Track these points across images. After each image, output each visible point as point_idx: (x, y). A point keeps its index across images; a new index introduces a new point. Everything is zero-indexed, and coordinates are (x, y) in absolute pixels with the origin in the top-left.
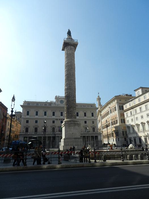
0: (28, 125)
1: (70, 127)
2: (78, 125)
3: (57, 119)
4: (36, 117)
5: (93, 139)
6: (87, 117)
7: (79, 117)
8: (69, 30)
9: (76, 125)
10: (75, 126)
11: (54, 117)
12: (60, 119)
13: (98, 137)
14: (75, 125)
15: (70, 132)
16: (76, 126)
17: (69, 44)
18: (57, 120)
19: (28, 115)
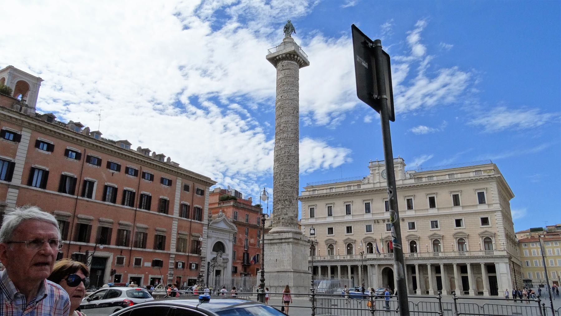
2: (287, 241)
3: (377, 221)
6: (463, 207)
7: (438, 209)
9: (283, 241)
10: (282, 243)
11: (368, 216)
12: (384, 221)
13: (496, 266)
14: (280, 241)
15: (272, 259)
16: (283, 244)
18: (378, 222)
19: (369, 212)
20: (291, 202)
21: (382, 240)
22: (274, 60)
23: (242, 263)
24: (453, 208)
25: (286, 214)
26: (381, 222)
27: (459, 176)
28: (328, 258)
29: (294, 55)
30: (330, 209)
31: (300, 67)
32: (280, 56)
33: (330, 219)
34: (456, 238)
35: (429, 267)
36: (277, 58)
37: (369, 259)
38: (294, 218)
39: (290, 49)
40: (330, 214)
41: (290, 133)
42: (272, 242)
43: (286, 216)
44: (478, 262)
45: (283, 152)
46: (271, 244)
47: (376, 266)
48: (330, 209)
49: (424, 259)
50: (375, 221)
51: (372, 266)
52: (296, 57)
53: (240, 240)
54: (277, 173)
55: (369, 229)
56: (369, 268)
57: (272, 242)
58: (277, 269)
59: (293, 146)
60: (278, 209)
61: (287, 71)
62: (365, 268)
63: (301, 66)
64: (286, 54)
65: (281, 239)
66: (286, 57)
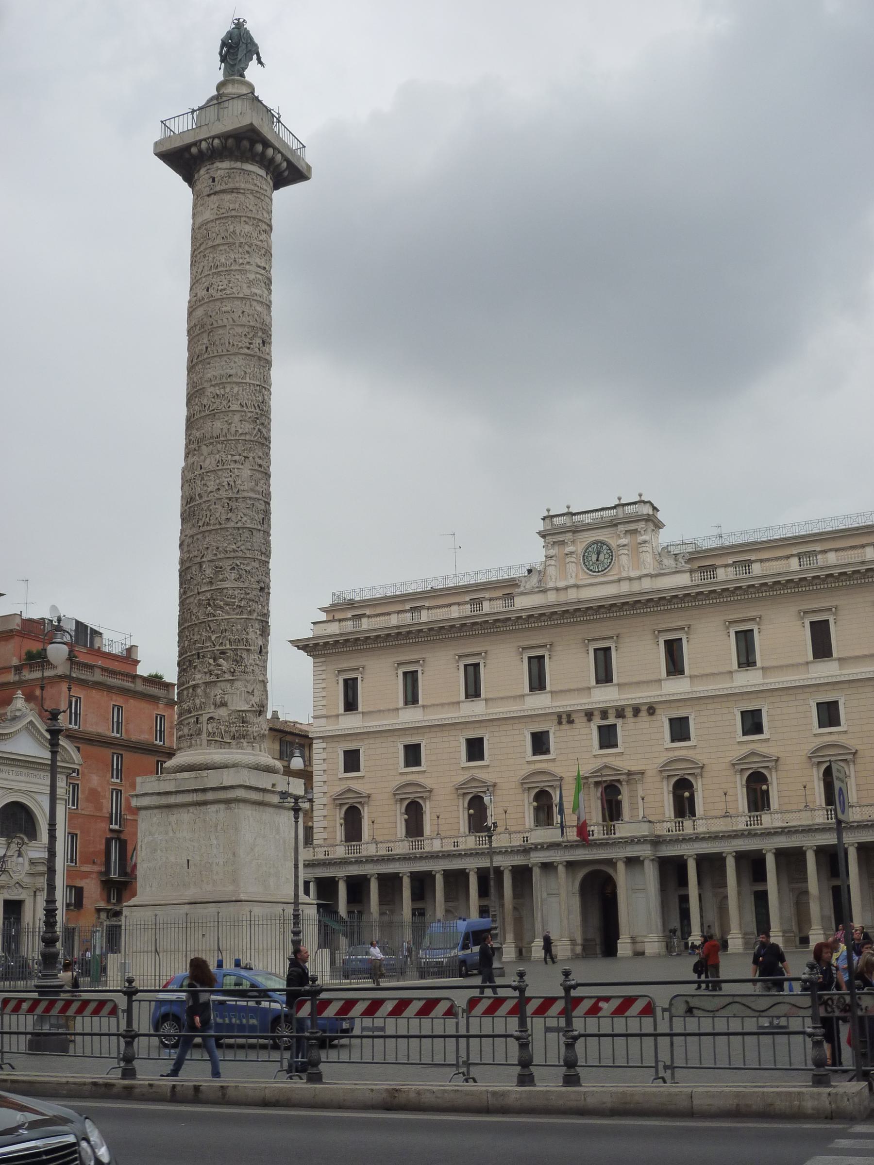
0: (356, 786)
1: (173, 818)
2: (222, 795)
3: (566, 718)
4: (411, 716)
5: (683, 882)
8: (239, 25)
9: (210, 796)
10: (205, 803)
11: (540, 702)
12: (589, 715)
14: (200, 797)
16: (212, 808)
17: (194, 150)
18: (570, 722)
20: (238, 661)
21: (581, 781)
22: (183, 158)
23: (100, 873)
24: (811, 666)
25: (224, 704)
26: (580, 720)
27: (832, 558)
28: (403, 847)
29: (253, 143)
30: (411, 680)
31: (277, 186)
32: (204, 145)
33: (411, 716)
34: (341, 805)
35: (730, 863)
36: (194, 150)
37: (537, 847)
38: (250, 717)
39: (234, 118)
40: (412, 698)
41: (237, 418)
42: (172, 800)
43: (223, 712)
44: (797, 844)
45: (212, 486)
46: (169, 806)
47: (561, 869)
48: (411, 680)
49: (715, 837)
50: (560, 717)
51: (547, 867)
52: (259, 148)
53: (94, 796)
54: (190, 559)
55: (540, 743)
56: (536, 872)
57: (172, 800)
58: (191, 893)
59: (248, 465)
60: (195, 687)
61: (228, 197)
62: (522, 875)
63: (280, 182)
64: (224, 137)
65: (204, 790)
66: (224, 147)
